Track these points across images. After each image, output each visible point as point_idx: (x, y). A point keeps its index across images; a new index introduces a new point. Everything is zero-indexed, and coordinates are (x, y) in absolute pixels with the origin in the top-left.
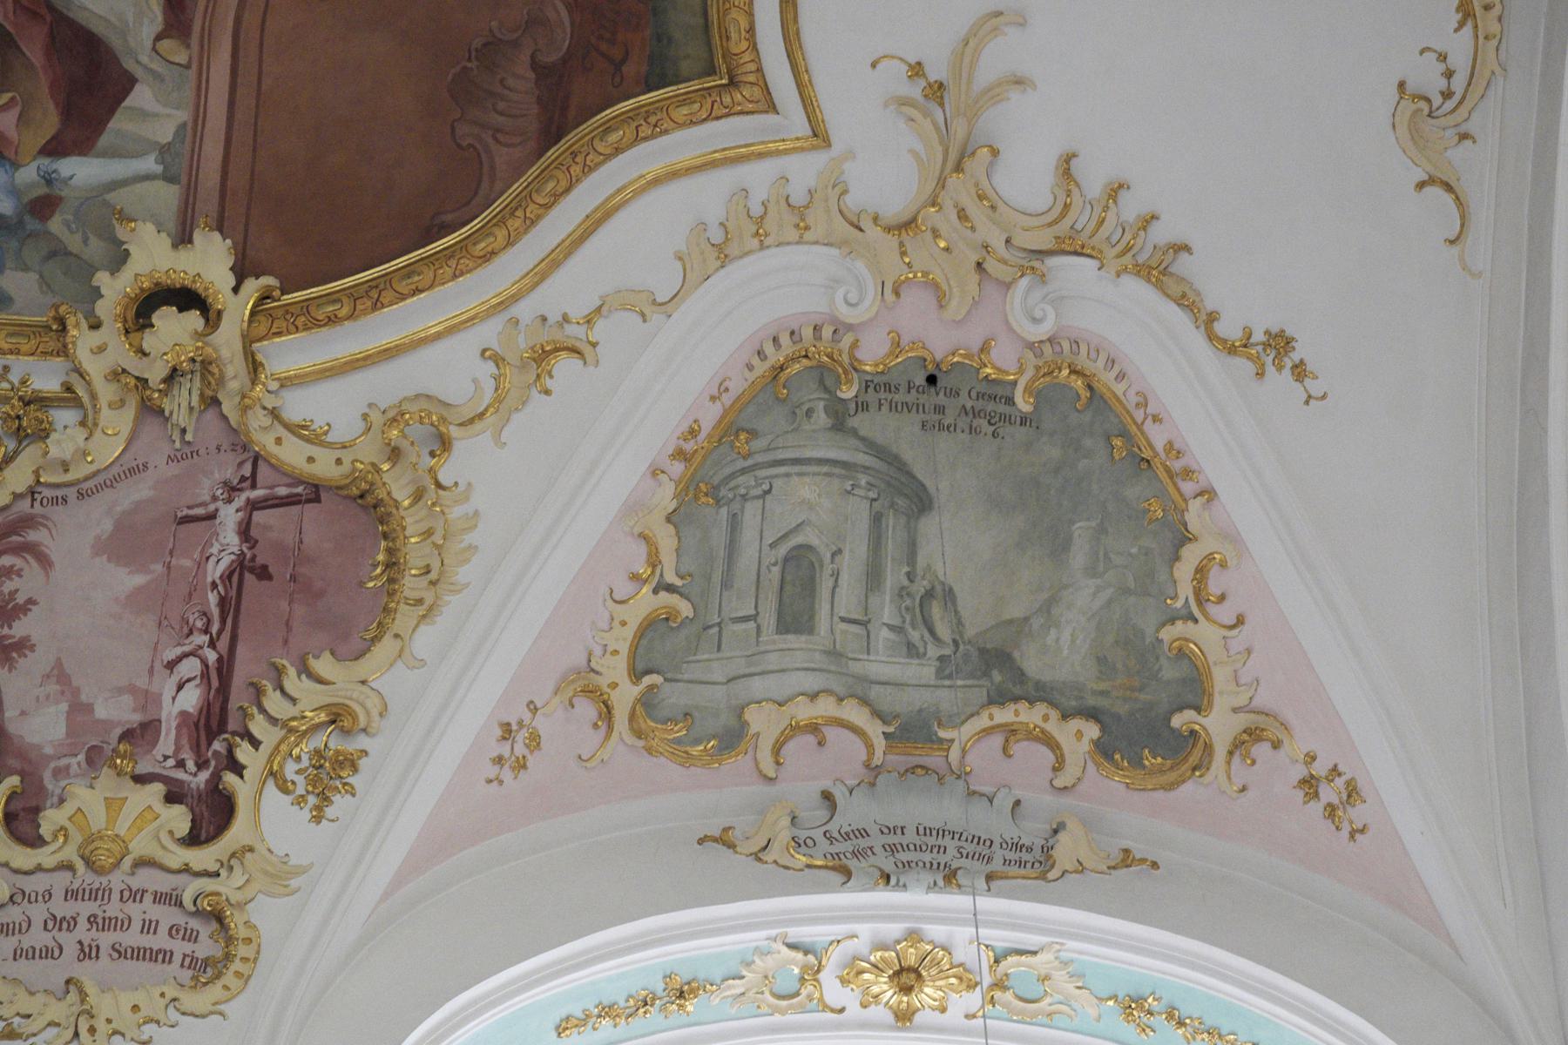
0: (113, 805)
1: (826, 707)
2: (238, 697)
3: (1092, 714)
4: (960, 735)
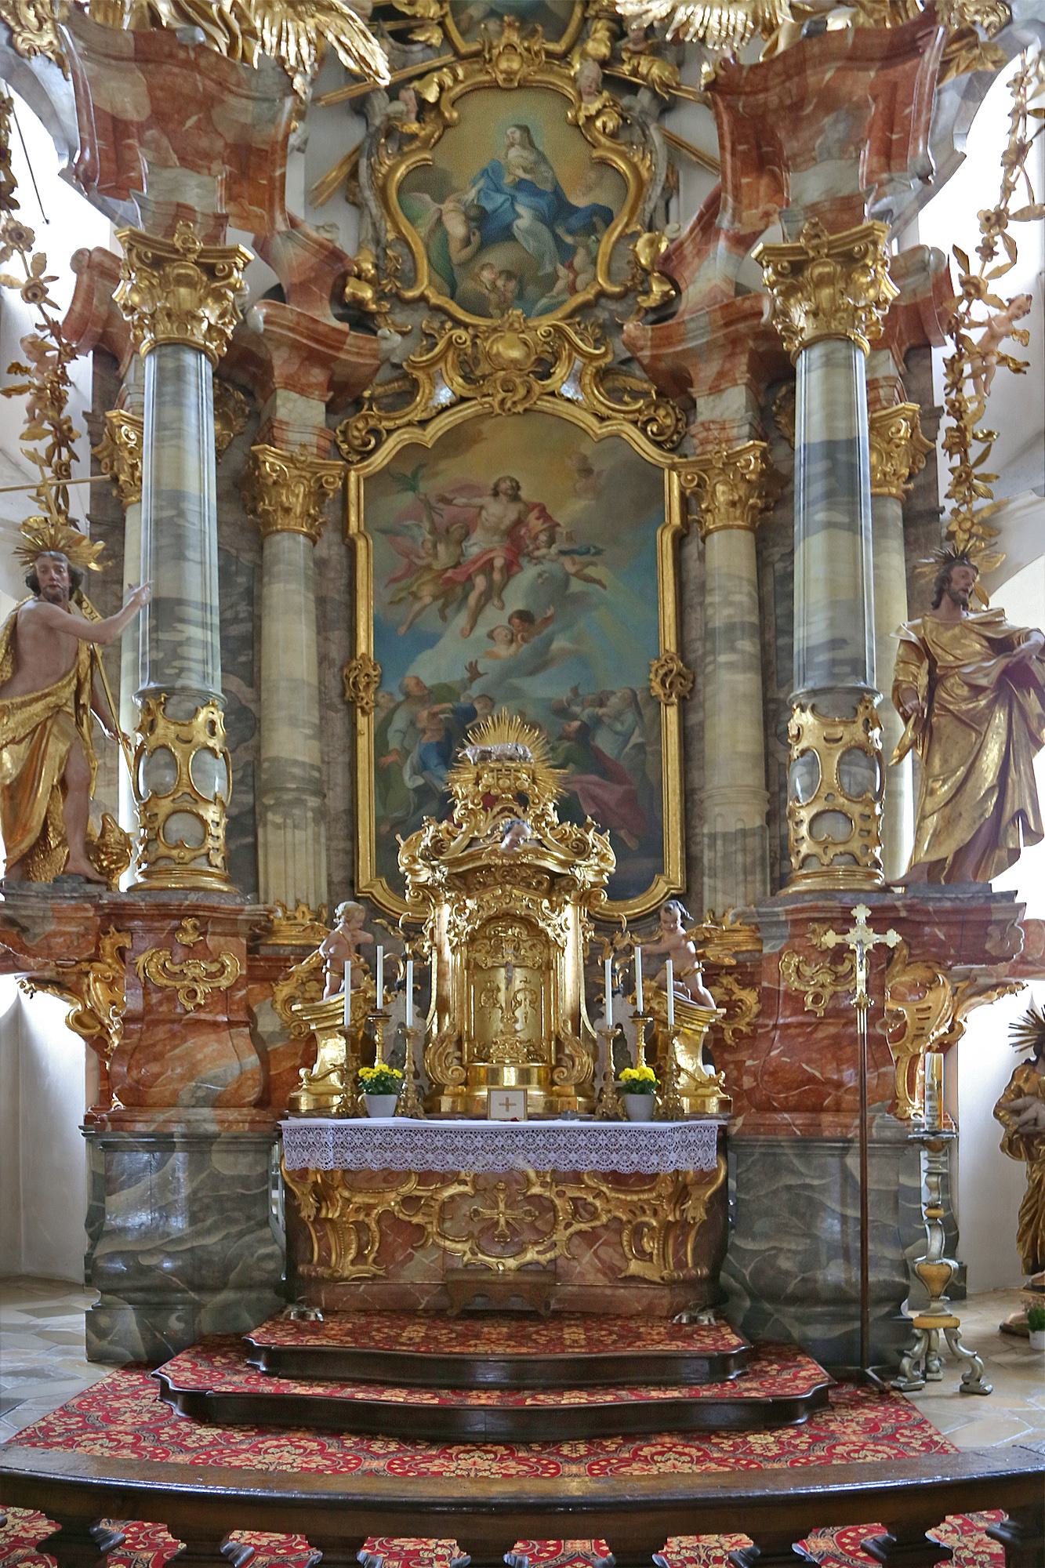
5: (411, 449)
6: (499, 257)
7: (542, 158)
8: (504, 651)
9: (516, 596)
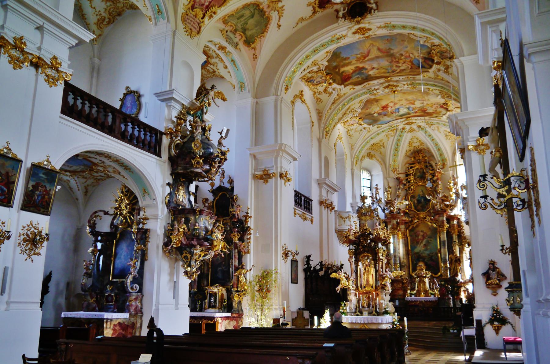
0: (199, 12)
1: (233, 25)
2: (210, 6)
3: (246, 38)
4: (238, 32)
5: (413, 227)
6: (420, 205)
7: (424, 193)
8: (423, 248)
9: (424, 243)
